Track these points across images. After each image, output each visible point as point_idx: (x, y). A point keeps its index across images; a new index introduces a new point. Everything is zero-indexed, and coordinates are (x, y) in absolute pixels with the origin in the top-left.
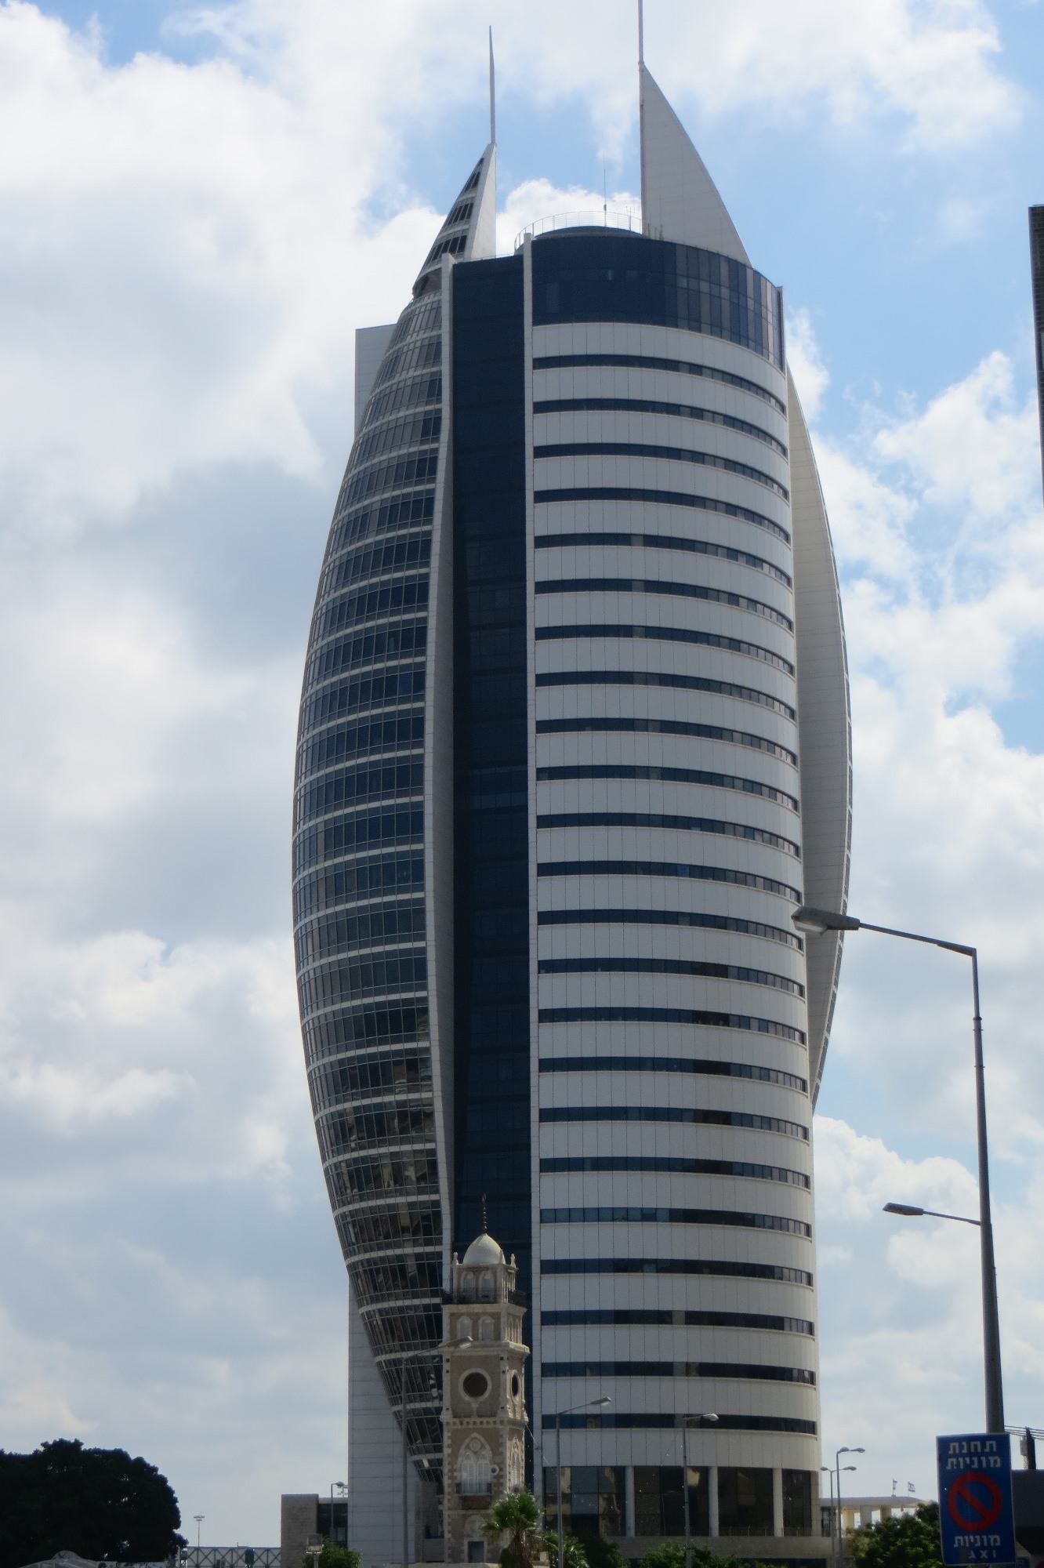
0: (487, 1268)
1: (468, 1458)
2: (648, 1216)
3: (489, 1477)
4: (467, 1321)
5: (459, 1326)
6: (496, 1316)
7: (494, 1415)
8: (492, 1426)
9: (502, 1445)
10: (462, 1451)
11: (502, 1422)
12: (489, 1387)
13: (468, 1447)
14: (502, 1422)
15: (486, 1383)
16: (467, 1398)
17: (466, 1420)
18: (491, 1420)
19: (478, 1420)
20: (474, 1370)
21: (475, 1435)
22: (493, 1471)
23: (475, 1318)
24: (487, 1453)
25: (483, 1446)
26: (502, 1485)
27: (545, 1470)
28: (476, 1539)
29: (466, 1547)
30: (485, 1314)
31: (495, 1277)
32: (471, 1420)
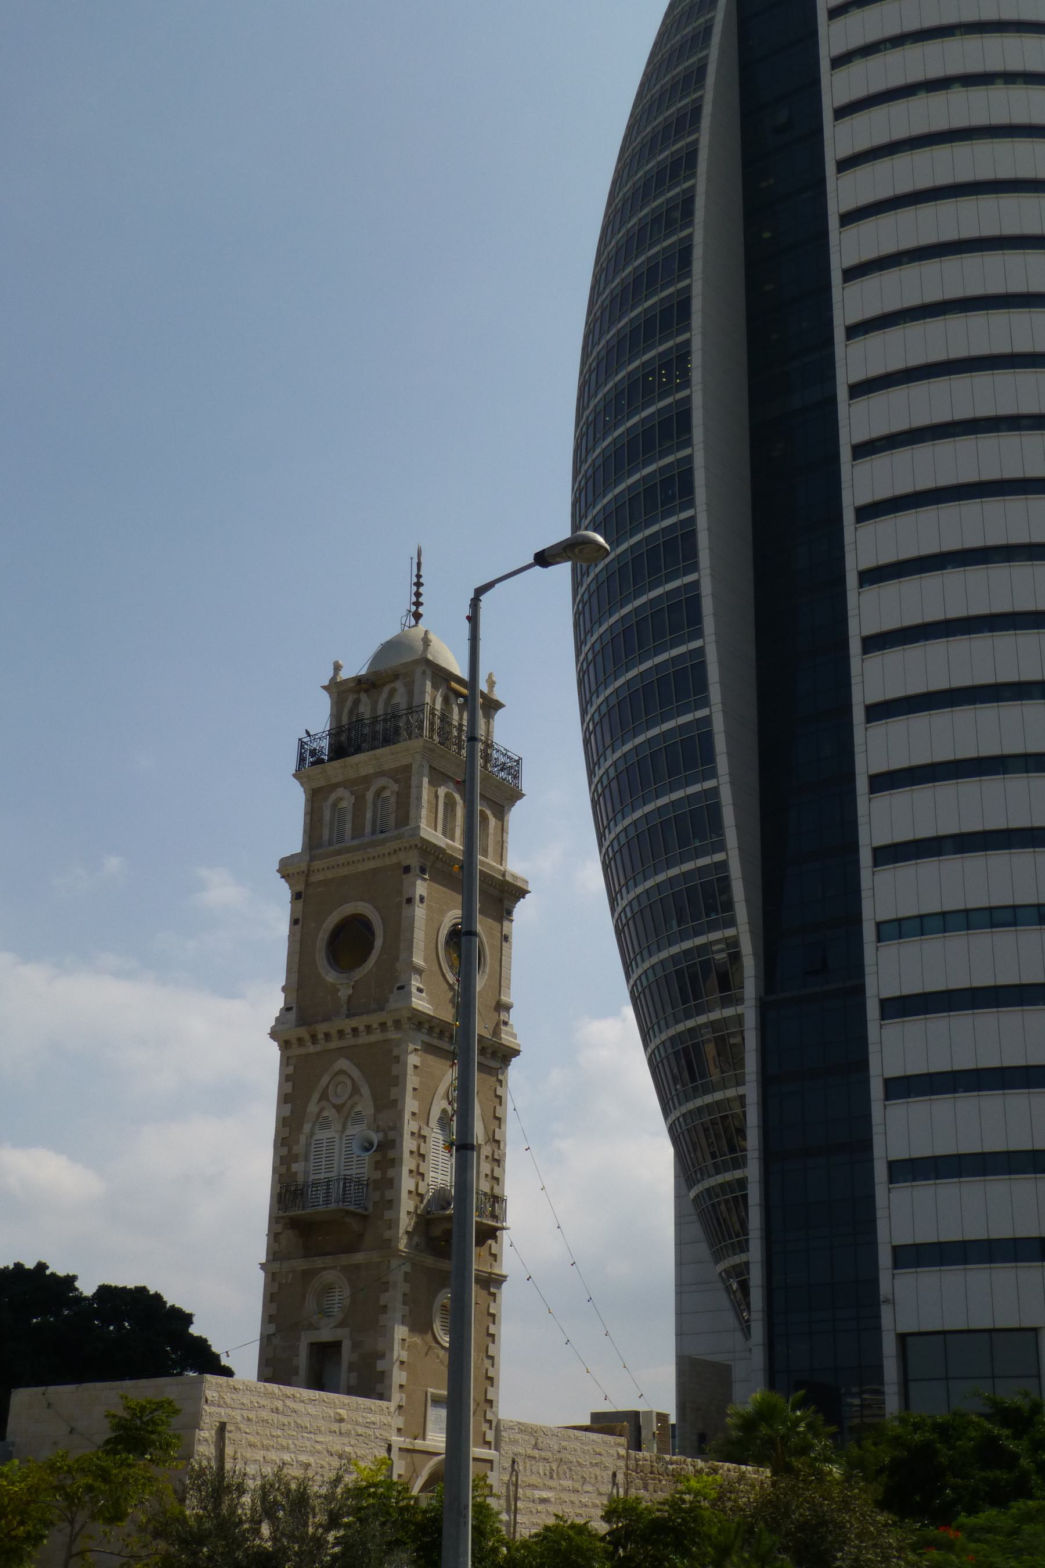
0: (396, 677)
1: (325, 1124)
3: (363, 1167)
5: (327, 816)
6: (403, 775)
7: (381, 1006)
8: (376, 1037)
9: (398, 1081)
10: (313, 1108)
11: (397, 1024)
12: (378, 943)
13: (324, 1096)
14: (397, 1024)
16: (331, 977)
17: (321, 1028)
18: (374, 1019)
19: (348, 1024)
20: (349, 909)
21: (343, 1064)
22: (367, 1147)
23: (358, 785)
24: (365, 1106)
25: (356, 1090)
26: (388, 1184)
27: (902, 1339)
28: (326, 1335)
29: (302, 1359)
30: (381, 774)
31: (410, 694)
32: (332, 1027)
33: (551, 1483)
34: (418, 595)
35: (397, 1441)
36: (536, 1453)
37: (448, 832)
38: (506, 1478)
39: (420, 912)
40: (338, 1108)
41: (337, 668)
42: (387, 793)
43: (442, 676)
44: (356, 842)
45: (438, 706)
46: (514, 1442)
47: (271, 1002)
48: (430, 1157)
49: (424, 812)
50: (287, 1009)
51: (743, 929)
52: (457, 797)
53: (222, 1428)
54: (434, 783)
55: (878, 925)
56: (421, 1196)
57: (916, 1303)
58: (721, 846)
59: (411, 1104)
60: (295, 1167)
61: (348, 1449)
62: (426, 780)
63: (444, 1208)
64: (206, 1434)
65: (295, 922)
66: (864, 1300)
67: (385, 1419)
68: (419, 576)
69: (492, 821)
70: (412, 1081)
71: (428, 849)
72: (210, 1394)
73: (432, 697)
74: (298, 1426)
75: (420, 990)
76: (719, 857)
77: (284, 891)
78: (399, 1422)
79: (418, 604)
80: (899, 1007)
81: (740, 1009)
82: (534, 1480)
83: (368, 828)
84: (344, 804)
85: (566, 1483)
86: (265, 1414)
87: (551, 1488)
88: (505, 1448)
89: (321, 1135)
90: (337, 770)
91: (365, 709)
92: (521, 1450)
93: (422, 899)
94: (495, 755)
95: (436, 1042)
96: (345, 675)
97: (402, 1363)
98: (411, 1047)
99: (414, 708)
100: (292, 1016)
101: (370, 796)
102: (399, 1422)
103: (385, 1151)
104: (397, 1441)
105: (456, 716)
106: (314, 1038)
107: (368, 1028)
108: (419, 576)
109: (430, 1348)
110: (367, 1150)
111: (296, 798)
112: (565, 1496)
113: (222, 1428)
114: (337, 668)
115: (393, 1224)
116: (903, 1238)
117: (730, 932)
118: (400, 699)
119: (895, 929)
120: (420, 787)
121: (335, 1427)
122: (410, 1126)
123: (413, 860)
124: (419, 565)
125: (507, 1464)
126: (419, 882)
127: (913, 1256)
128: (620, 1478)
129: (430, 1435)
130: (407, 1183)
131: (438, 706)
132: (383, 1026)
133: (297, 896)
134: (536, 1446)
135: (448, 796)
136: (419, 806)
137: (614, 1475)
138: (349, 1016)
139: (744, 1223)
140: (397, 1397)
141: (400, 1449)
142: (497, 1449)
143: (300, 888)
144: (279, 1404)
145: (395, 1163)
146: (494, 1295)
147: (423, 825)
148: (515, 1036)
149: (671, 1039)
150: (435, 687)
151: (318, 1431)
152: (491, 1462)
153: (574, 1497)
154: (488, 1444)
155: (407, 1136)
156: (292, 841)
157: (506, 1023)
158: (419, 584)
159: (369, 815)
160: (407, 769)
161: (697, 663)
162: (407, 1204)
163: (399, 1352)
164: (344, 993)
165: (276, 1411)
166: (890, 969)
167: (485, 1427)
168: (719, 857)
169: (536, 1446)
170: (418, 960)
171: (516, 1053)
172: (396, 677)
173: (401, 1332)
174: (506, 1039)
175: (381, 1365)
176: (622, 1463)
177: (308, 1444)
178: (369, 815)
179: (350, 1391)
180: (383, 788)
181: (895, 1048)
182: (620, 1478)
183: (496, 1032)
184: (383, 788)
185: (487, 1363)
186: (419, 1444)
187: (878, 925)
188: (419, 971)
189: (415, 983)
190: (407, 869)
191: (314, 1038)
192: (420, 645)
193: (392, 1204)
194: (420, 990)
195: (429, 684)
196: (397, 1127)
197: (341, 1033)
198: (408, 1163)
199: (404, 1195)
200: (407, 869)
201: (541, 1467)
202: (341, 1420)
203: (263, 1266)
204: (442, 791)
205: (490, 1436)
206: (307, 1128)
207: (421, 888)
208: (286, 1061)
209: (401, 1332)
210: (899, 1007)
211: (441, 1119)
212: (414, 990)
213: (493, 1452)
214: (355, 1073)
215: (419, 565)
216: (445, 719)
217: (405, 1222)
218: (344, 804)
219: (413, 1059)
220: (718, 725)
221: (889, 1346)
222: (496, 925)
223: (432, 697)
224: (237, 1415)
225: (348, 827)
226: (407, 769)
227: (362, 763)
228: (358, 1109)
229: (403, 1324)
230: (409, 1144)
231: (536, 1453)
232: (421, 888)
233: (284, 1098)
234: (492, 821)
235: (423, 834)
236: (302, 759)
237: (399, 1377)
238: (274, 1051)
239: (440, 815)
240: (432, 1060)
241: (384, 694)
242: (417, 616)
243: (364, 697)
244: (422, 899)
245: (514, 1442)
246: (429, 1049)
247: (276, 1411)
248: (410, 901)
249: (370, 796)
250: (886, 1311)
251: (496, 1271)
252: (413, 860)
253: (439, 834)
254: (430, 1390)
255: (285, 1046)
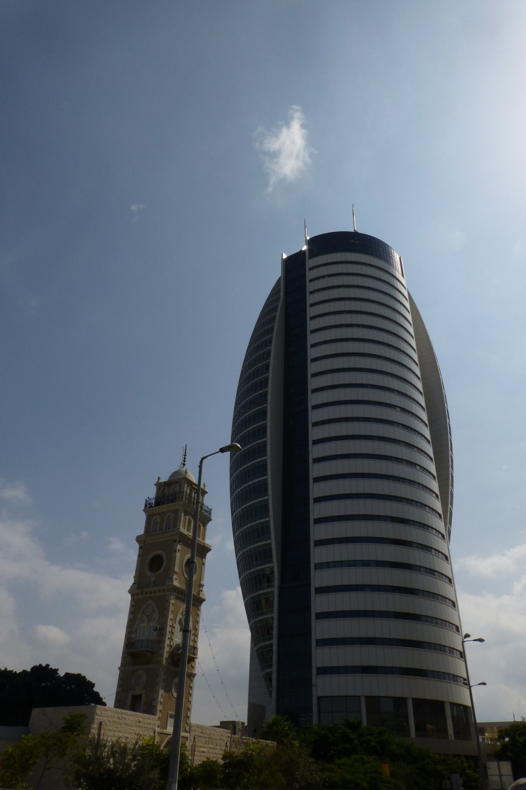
0: (176, 482)
2: (366, 563)
4: (158, 519)
6: (176, 512)
9: (167, 608)
10: (139, 616)
12: (164, 564)
14: (168, 590)
15: (163, 561)
16: (149, 574)
20: (156, 552)
21: (150, 602)
26: (161, 642)
27: (319, 698)
28: (137, 692)
33: (206, 746)
34: (185, 458)
35: (158, 730)
36: (202, 735)
37: (188, 530)
38: (191, 744)
39: (178, 555)
40: (148, 616)
41: (159, 479)
42: (171, 517)
43: (190, 483)
44: (160, 532)
45: (188, 492)
46: (195, 731)
47: (130, 581)
48: (175, 634)
49: (182, 523)
50: (134, 583)
51: (275, 564)
52: (192, 519)
53: (101, 724)
54: (185, 515)
55: (315, 564)
56: (171, 646)
57: (324, 686)
58: (270, 538)
59: (171, 616)
60: (132, 635)
61: (141, 732)
62: (183, 514)
63: (178, 651)
64: (95, 726)
65: (139, 556)
66: (307, 685)
67: (155, 722)
68: (185, 453)
69: (202, 527)
70: (171, 608)
71: (182, 535)
72: (98, 712)
73: (186, 489)
74: (126, 724)
75: (176, 579)
76: (269, 541)
77: (137, 546)
78: (158, 723)
79: (184, 461)
80: (321, 590)
81: (273, 589)
82: (201, 744)
83: (164, 528)
84: (158, 520)
85: (211, 746)
86: (115, 719)
87: (206, 748)
88: (193, 733)
89: (142, 625)
90: (156, 510)
91: (166, 491)
92: (197, 734)
93: (179, 551)
94: (204, 507)
95: (180, 596)
96: (161, 481)
97: (161, 703)
98: (172, 597)
99: (181, 492)
100: (136, 586)
101: (165, 518)
102: (158, 723)
103: (161, 631)
104: (158, 730)
105: (193, 495)
106: (142, 593)
107: (159, 591)
108: (185, 453)
109: (170, 698)
110: (156, 630)
111: (143, 518)
112: (210, 750)
113: (101, 724)
114: (159, 479)
115: (162, 655)
116: (320, 665)
117: (271, 565)
118: (177, 489)
119: (320, 566)
120: (181, 516)
121: (138, 724)
122: (170, 623)
123: (177, 538)
124: (186, 450)
125: (192, 739)
126: (178, 545)
127: (324, 671)
128: (228, 744)
129: (168, 728)
130: (167, 642)
131: (188, 492)
132: (164, 590)
133: (141, 548)
134: (202, 733)
135: (189, 519)
136: (180, 522)
137: (226, 743)
138: (154, 586)
139: (271, 659)
140: (159, 714)
141: (158, 733)
142: (189, 733)
143: (142, 545)
144: (120, 716)
145: (164, 635)
146: (192, 680)
147: (181, 527)
148: (204, 595)
149: (252, 598)
150: (188, 486)
151: (132, 726)
152: (187, 738)
153: (213, 751)
154: (186, 731)
155: (168, 626)
156: (141, 530)
157: (202, 591)
158: (185, 455)
159: (165, 524)
160: (177, 511)
161: (265, 482)
162: (167, 649)
163: (160, 699)
164: (153, 579)
165: (119, 718)
166: (319, 579)
167: (186, 726)
168: (269, 541)
169: (202, 733)
170: (176, 570)
171: (204, 600)
172: (176, 482)
173: (161, 692)
174: (201, 596)
175: (154, 703)
176: (229, 739)
177: (128, 730)
178: (165, 524)
179: (144, 712)
180: (170, 516)
181: (320, 603)
182: (228, 744)
183: (199, 593)
184: (170, 516)
185: (188, 703)
186: (164, 731)
187: (315, 564)
188: (176, 573)
189: (175, 577)
190: (175, 541)
191: (142, 593)
192: (184, 473)
193: (162, 648)
194: (176, 579)
195: (186, 485)
196: (165, 623)
197: (151, 592)
198: (168, 635)
199: (166, 646)
200: (175, 541)
201: (203, 740)
202: (140, 722)
203: (119, 668)
204: (187, 518)
205: (187, 729)
206: (137, 622)
207: (179, 547)
208: (132, 600)
209: (161, 692)
210: (321, 590)
211: (179, 621)
212: (174, 579)
213: (188, 734)
214: (154, 605)
215: (186, 450)
216: (190, 495)
217: (166, 655)
218: (158, 520)
219: (172, 601)
220: (270, 501)
221: (315, 701)
222: (201, 560)
223: (186, 489)
224: (106, 719)
225: (158, 527)
226: (177, 511)
227: (164, 508)
228: (154, 617)
229: (162, 689)
230: (169, 629)
231: (202, 735)
232: (179, 547)
233: (131, 613)
234: (202, 527)
235: (181, 530)
236: (146, 506)
237: (160, 707)
238: (129, 597)
239: (186, 525)
240: (178, 602)
241: (172, 487)
242: (184, 465)
243: (166, 488)
244: (179, 551)
245: (195, 731)
246: (178, 598)
247: (119, 718)
248: (175, 551)
249: (165, 518)
250: (314, 689)
251: (193, 672)
252: (177, 538)
253: (186, 530)
254: (169, 712)
255: (133, 595)
